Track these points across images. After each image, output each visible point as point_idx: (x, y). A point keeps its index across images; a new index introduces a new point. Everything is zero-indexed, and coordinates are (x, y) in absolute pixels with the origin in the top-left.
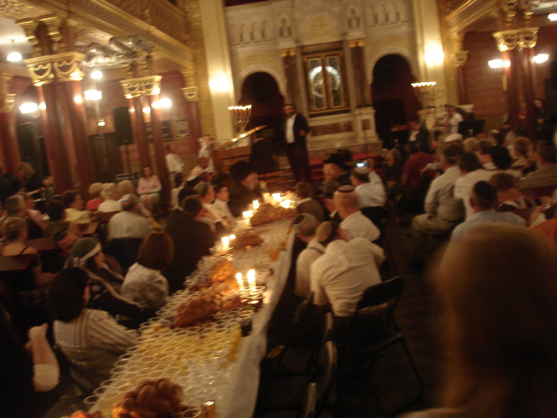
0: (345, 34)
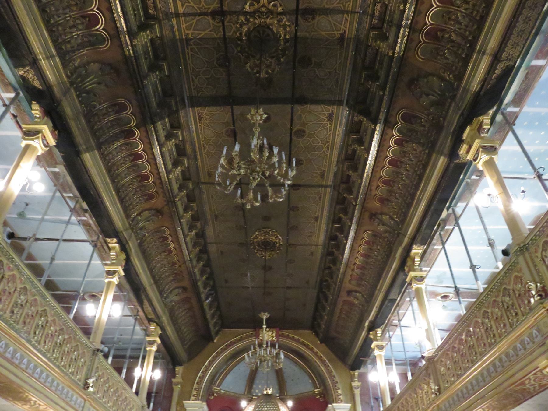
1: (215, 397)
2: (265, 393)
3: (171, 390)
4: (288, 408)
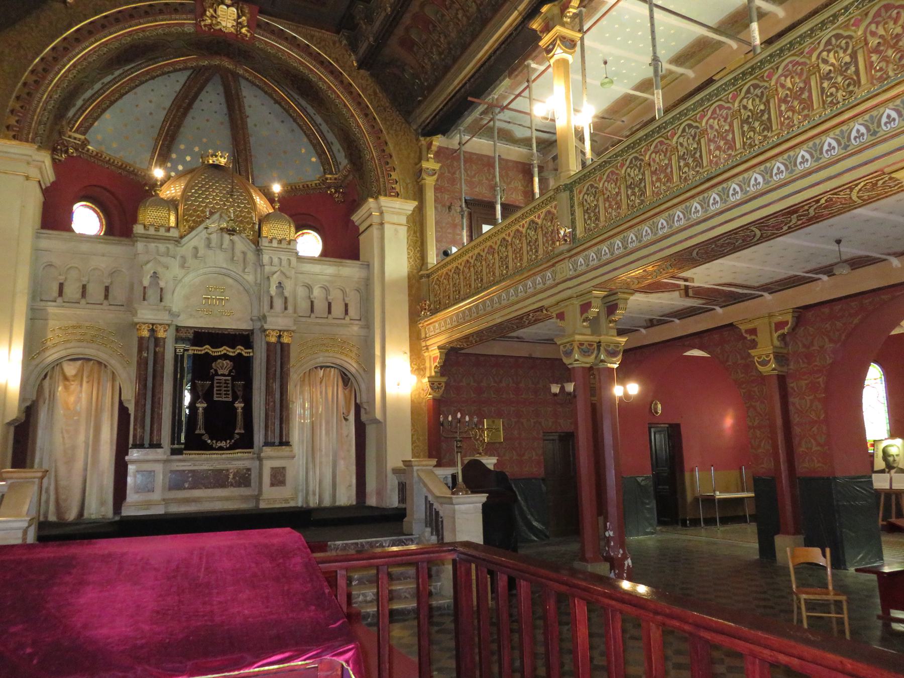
1: (70, 157)
2: (211, 162)
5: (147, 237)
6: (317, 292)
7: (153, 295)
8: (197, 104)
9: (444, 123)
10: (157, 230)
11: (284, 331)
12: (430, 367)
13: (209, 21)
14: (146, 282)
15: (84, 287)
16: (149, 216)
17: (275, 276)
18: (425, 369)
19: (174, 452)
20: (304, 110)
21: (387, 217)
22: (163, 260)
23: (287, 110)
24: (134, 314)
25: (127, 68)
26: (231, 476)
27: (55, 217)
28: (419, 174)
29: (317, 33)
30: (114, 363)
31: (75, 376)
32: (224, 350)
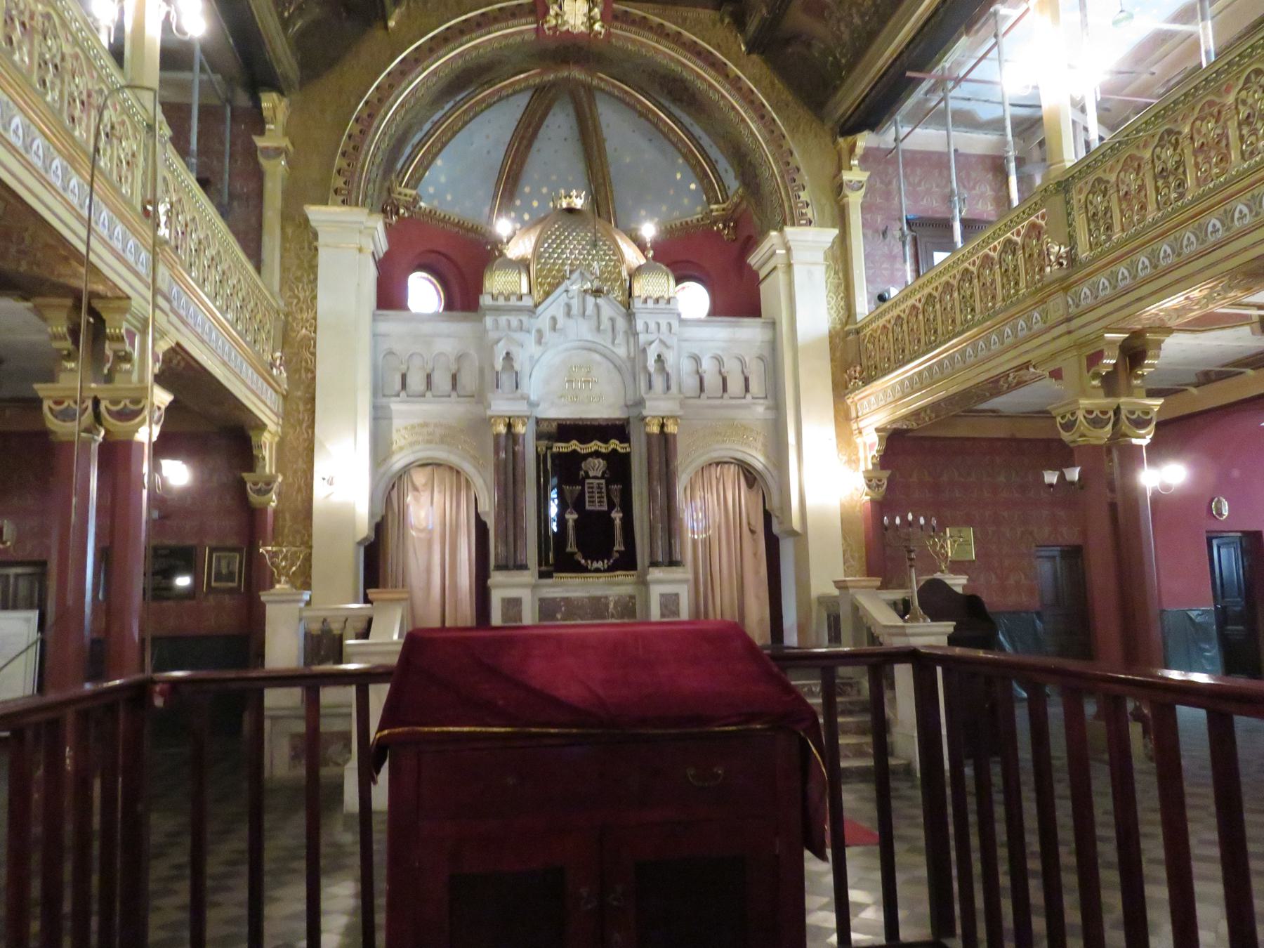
0: (640, 403)
1: (401, 219)
2: (564, 206)
3: (258, 175)
4: (642, 247)
5: (497, 310)
6: (707, 365)
7: (506, 380)
8: (542, 132)
9: (873, 113)
10: (507, 299)
11: (668, 418)
12: (866, 458)
13: (554, 22)
14: (499, 364)
15: (429, 377)
16: (498, 283)
17: (653, 345)
18: (858, 460)
19: (542, 575)
20: (677, 121)
21: (797, 257)
22: (519, 336)
23: (656, 124)
24: (489, 406)
25: (458, 98)
26: (611, 605)
27: (390, 296)
28: (838, 189)
29: (691, 13)
30: (468, 468)
31: (425, 485)
32: (595, 445)
